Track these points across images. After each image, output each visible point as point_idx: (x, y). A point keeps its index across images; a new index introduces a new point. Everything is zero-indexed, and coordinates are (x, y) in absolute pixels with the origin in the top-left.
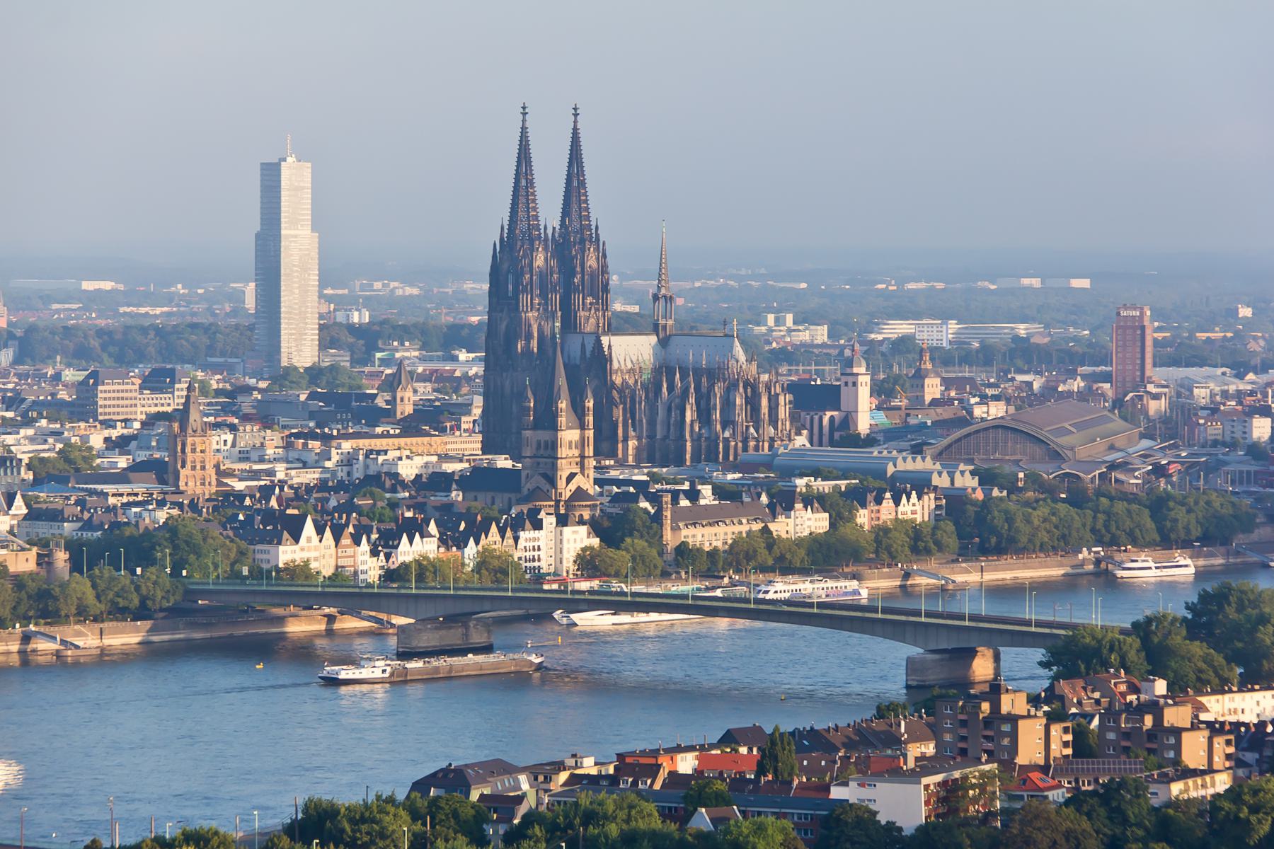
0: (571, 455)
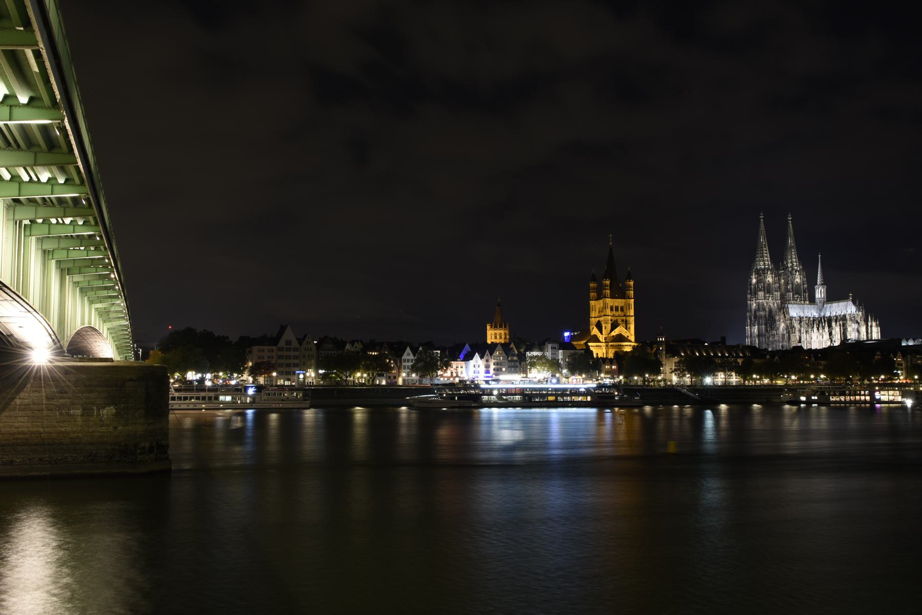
0: (617, 315)
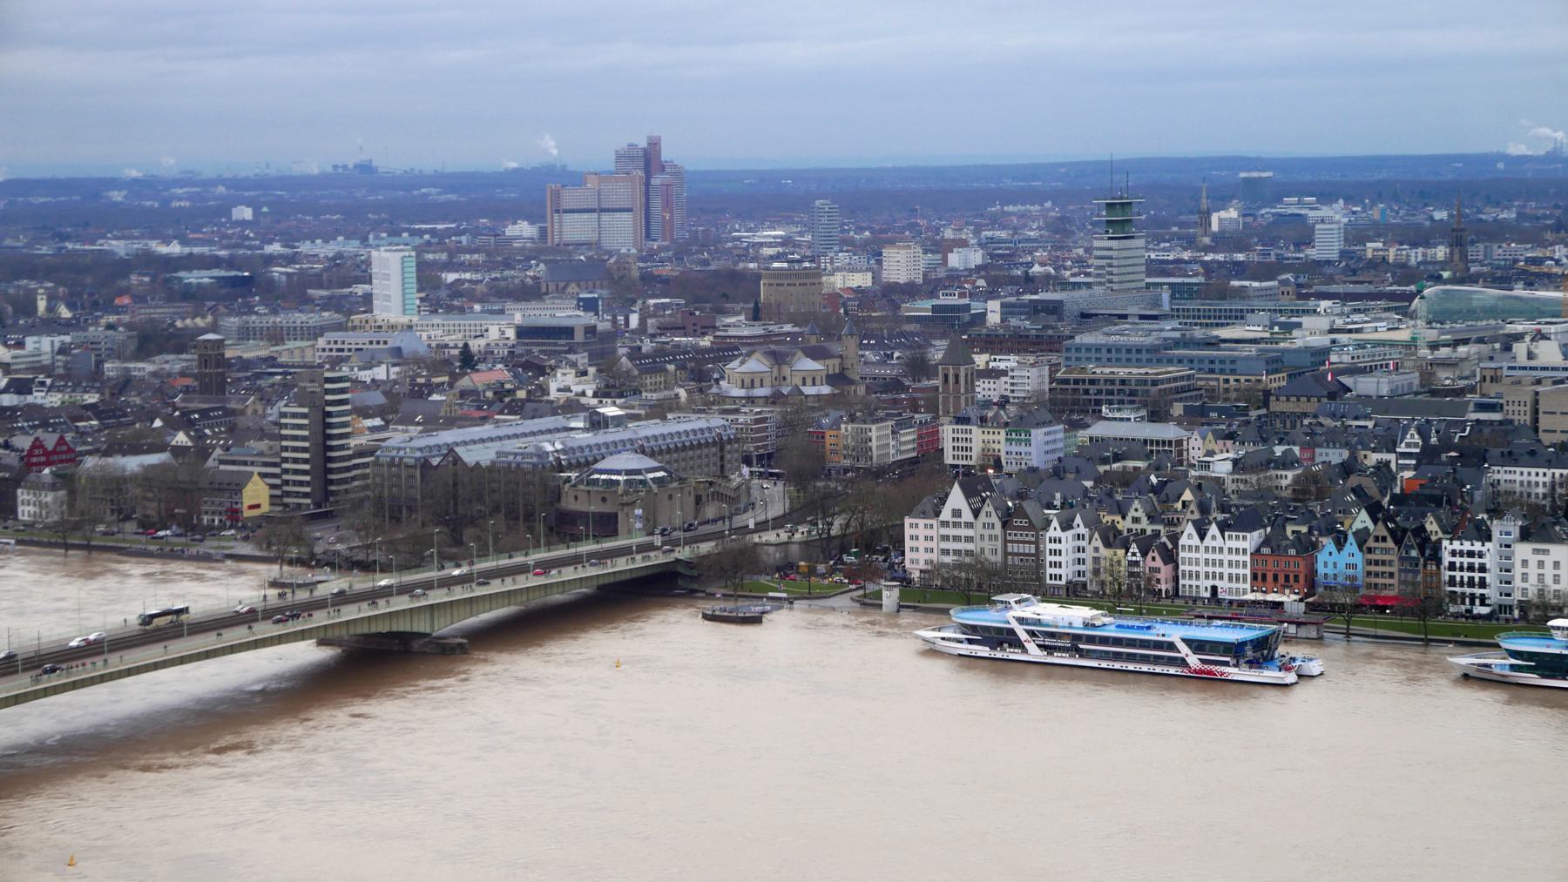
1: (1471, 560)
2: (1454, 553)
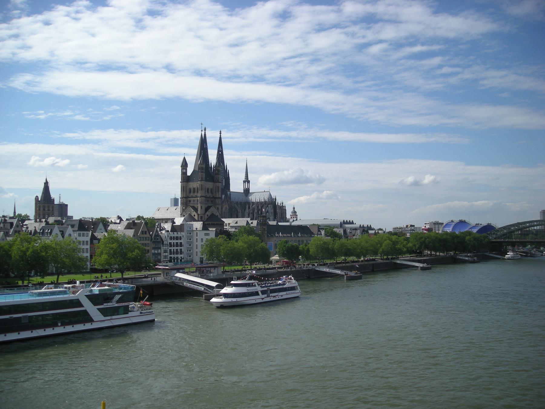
0: (208, 196)
1: (177, 241)
2: (171, 238)
